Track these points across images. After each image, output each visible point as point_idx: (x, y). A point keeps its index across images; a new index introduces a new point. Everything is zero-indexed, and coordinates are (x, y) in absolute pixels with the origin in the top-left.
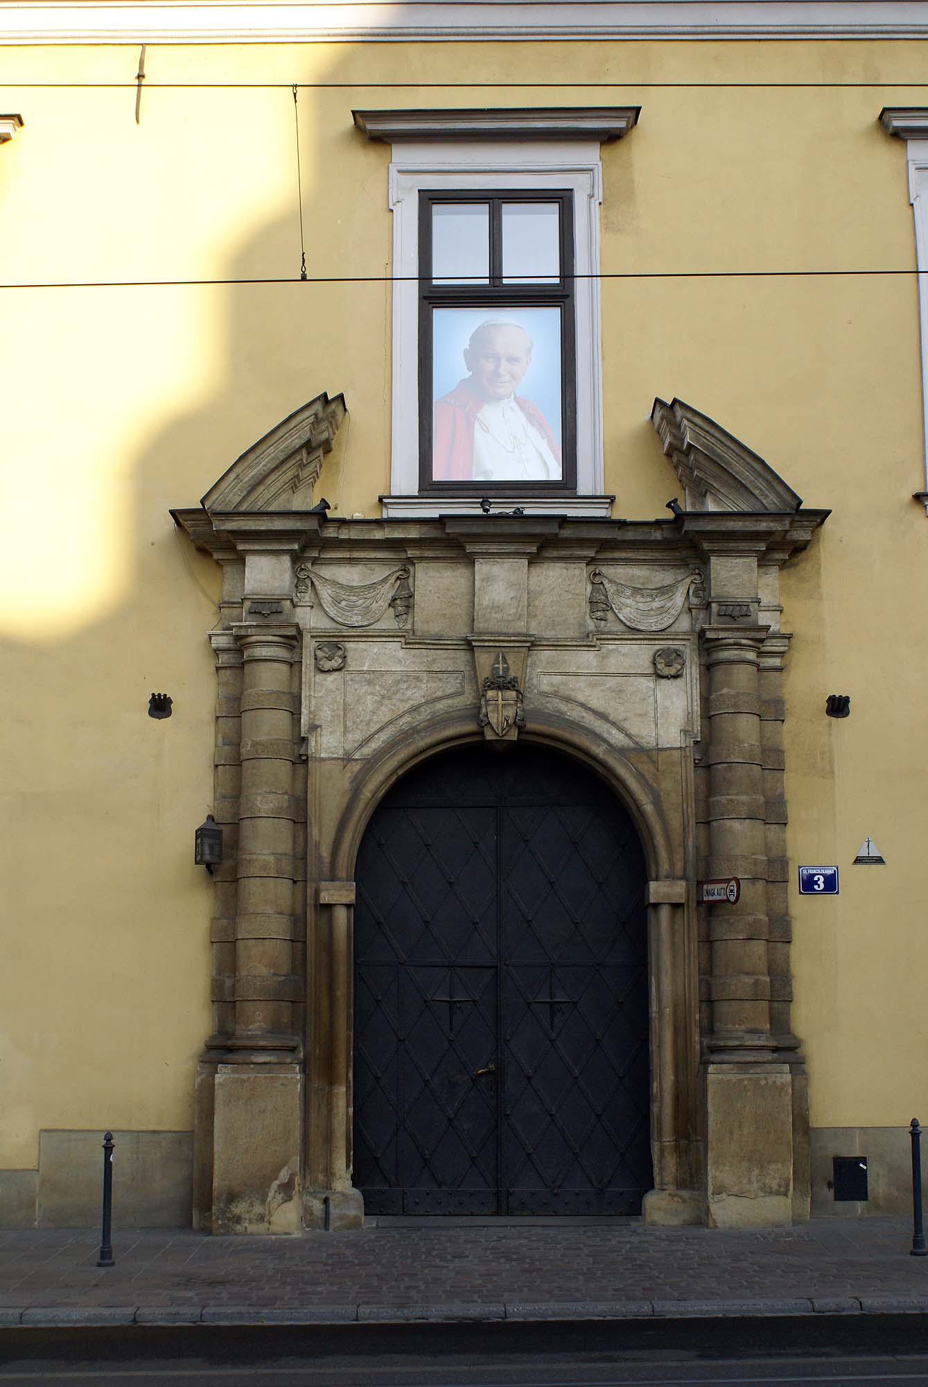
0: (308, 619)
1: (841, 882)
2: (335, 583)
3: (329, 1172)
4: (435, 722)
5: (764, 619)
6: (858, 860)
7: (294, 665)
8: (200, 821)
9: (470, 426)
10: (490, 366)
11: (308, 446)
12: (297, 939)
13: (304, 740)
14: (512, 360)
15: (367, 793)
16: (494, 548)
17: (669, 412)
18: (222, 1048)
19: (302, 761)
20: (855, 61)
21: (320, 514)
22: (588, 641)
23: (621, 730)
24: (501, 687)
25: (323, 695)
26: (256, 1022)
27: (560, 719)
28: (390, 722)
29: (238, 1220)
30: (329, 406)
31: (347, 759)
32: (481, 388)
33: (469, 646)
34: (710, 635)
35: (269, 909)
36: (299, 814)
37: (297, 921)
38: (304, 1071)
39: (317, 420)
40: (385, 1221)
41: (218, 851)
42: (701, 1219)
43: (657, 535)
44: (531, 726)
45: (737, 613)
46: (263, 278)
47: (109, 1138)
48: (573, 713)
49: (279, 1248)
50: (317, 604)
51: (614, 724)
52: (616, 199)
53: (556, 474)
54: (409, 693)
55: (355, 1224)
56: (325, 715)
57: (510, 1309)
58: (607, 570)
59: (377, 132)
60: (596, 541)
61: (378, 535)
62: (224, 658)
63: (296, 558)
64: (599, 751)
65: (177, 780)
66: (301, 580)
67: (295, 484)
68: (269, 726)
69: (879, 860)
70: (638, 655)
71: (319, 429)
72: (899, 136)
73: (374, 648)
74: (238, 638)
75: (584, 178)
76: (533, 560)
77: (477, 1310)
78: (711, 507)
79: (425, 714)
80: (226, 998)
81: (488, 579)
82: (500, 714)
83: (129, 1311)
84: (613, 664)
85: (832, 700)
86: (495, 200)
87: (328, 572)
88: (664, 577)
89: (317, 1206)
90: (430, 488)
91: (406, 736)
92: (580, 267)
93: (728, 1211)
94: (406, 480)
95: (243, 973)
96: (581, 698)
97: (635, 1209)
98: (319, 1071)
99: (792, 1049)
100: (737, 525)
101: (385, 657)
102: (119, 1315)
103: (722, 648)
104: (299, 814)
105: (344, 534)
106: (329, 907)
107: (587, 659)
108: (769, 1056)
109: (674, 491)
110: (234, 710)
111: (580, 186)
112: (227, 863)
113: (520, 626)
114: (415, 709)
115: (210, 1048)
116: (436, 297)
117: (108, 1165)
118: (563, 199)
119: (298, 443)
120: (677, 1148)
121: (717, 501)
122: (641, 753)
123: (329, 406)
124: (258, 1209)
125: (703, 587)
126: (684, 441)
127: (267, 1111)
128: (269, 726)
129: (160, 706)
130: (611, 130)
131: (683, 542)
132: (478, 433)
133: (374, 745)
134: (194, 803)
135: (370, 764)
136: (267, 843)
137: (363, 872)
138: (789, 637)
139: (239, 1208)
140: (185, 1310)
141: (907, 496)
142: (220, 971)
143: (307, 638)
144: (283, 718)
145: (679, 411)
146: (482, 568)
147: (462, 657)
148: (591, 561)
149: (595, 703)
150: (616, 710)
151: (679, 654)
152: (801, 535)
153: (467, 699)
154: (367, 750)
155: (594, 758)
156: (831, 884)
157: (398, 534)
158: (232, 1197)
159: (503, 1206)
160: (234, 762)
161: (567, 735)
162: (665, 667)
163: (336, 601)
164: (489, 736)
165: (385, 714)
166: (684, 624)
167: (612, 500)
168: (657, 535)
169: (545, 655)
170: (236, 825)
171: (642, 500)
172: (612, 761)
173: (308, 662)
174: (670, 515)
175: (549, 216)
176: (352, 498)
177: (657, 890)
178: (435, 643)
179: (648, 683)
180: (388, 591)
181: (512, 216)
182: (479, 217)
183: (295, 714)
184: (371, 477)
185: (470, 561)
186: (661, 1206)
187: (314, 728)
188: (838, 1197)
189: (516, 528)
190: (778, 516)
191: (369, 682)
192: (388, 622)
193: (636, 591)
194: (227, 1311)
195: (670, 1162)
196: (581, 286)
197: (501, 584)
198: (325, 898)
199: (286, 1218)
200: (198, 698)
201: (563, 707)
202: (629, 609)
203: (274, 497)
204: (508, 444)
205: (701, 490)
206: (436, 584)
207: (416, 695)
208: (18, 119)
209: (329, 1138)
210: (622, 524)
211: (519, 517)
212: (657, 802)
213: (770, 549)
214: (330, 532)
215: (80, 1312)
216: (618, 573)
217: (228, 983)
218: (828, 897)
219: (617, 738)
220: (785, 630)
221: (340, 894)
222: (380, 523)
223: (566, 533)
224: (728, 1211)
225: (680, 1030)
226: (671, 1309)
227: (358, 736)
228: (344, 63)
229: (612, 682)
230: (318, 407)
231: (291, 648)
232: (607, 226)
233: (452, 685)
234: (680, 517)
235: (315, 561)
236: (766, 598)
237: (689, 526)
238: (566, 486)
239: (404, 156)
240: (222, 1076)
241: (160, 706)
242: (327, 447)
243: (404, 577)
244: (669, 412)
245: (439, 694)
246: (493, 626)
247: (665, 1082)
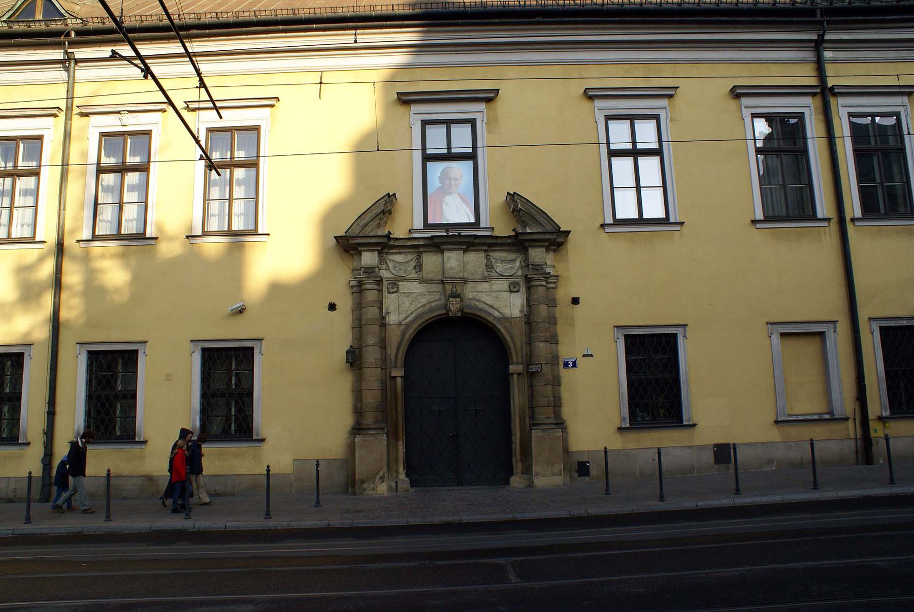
0: (385, 274)
2: (393, 261)
3: (397, 472)
4: (431, 310)
5: (548, 270)
6: (584, 356)
7: (380, 291)
8: (347, 348)
9: (441, 204)
10: (447, 182)
11: (383, 212)
12: (384, 389)
13: (384, 318)
14: (456, 179)
15: (407, 336)
16: (450, 247)
17: (513, 197)
18: (358, 429)
19: (383, 325)
20: (575, 71)
21: (388, 237)
22: (485, 279)
23: (498, 311)
24: (454, 297)
25: (390, 301)
26: (369, 419)
27: (476, 308)
29: (365, 490)
30: (390, 198)
31: (400, 324)
32: (445, 190)
33: (443, 282)
35: (373, 379)
36: (383, 344)
37: (384, 382)
38: (387, 436)
39: (386, 203)
40: (417, 489)
41: (354, 358)
42: (531, 485)
43: (509, 241)
44: (465, 311)
45: (539, 268)
46: (367, 151)
47: (318, 461)
48: (481, 306)
49: (381, 499)
50: (388, 269)
51: (496, 309)
52: (492, 122)
53: (473, 220)
55: (407, 490)
56: (391, 308)
57: (463, 518)
58: (492, 254)
59: (405, 100)
60: (486, 243)
61: (409, 243)
62: (355, 289)
63: (380, 253)
64: (490, 319)
65: (338, 333)
66: (382, 260)
67: (379, 226)
68: (372, 313)
69: (591, 356)
70: (504, 284)
71: (386, 206)
72: (591, 98)
73: (409, 284)
74: (360, 281)
75: (480, 114)
76: (465, 251)
77: (450, 519)
78: (529, 231)
79: (427, 307)
80: (358, 411)
81: (449, 258)
82: (454, 306)
83: (327, 522)
84: (495, 288)
85: (573, 298)
86: (448, 123)
87: (391, 257)
88: (512, 256)
89: (393, 484)
90: (427, 226)
92: (479, 144)
93: (541, 482)
94: (418, 224)
95: (364, 402)
97: (507, 482)
98: (393, 436)
99: (562, 424)
100: (538, 237)
101: (414, 287)
102: (323, 523)
103: (534, 281)
104: (383, 344)
105: (397, 244)
106: (395, 378)
107: (485, 286)
108: (554, 426)
109: (515, 225)
110: (358, 308)
111: (478, 116)
112: (358, 363)
113: (461, 275)
114: (424, 306)
115: (353, 429)
116: (427, 158)
117: (318, 471)
118: (473, 122)
119: (379, 211)
120: (522, 460)
121: (530, 228)
122: (505, 319)
123: (390, 198)
124: (372, 486)
125: (526, 259)
126: (518, 207)
127: (375, 451)
128: (372, 313)
129: (332, 307)
130: (489, 97)
131: (518, 244)
132: (444, 205)
133: (409, 319)
134: (344, 341)
135: (408, 326)
136: (371, 355)
137: (407, 364)
138: (557, 276)
139: (365, 486)
140: (347, 521)
141: (598, 225)
142: (356, 402)
143: (384, 281)
144: (376, 310)
145: (516, 197)
146: (447, 254)
147: (440, 287)
148: (486, 251)
149: (488, 302)
150: (497, 305)
151: (518, 284)
152: (561, 240)
153: (443, 302)
154: (407, 321)
155: (489, 322)
157: (416, 243)
158: (363, 482)
159: (460, 483)
160: (359, 326)
161: (479, 314)
162: (513, 288)
163: (394, 267)
164: (451, 315)
165: (413, 308)
166: (520, 273)
167: (493, 228)
168: (509, 241)
169: (470, 285)
170: (360, 349)
171: (503, 229)
172: (495, 323)
173: (385, 290)
174: (513, 234)
175: (468, 129)
176: (399, 230)
177: (512, 368)
178: (430, 281)
179: (508, 294)
180: (413, 264)
181: (455, 129)
182: (443, 129)
183: (381, 309)
184: (406, 222)
185: (442, 252)
186: (516, 481)
187: (388, 313)
188: (579, 476)
189: (458, 240)
190: (552, 233)
192: (413, 275)
193: (502, 261)
194: (362, 521)
195: (519, 465)
196: (480, 151)
197: (454, 260)
198: (393, 374)
199: (382, 489)
200: (345, 303)
201: (477, 303)
202: (500, 268)
203: (371, 230)
204: (455, 210)
205: (524, 224)
206: (430, 261)
207: (424, 301)
208: (277, 99)
209: (397, 460)
210: (497, 237)
211: (459, 235)
212: (512, 337)
213: (550, 245)
214: (392, 243)
215: (309, 522)
216: (495, 255)
217: (359, 406)
219: (496, 314)
220: (556, 274)
221: (398, 373)
222: (410, 239)
223: (477, 241)
224: (541, 482)
225: (522, 418)
226: (520, 516)
227: (404, 316)
228: (394, 75)
229: (494, 294)
230: (386, 198)
231: (379, 285)
232: (489, 132)
233: (437, 296)
234: (517, 234)
235: (386, 253)
236: (549, 263)
237: (520, 237)
238: (476, 225)
239: (415, 108)
240: (358, 439)
241: (332, 307)
242: (390, 212)
243: (419, 258)
244: (513, 197)
246: (451, 275)
247: (517, 436)
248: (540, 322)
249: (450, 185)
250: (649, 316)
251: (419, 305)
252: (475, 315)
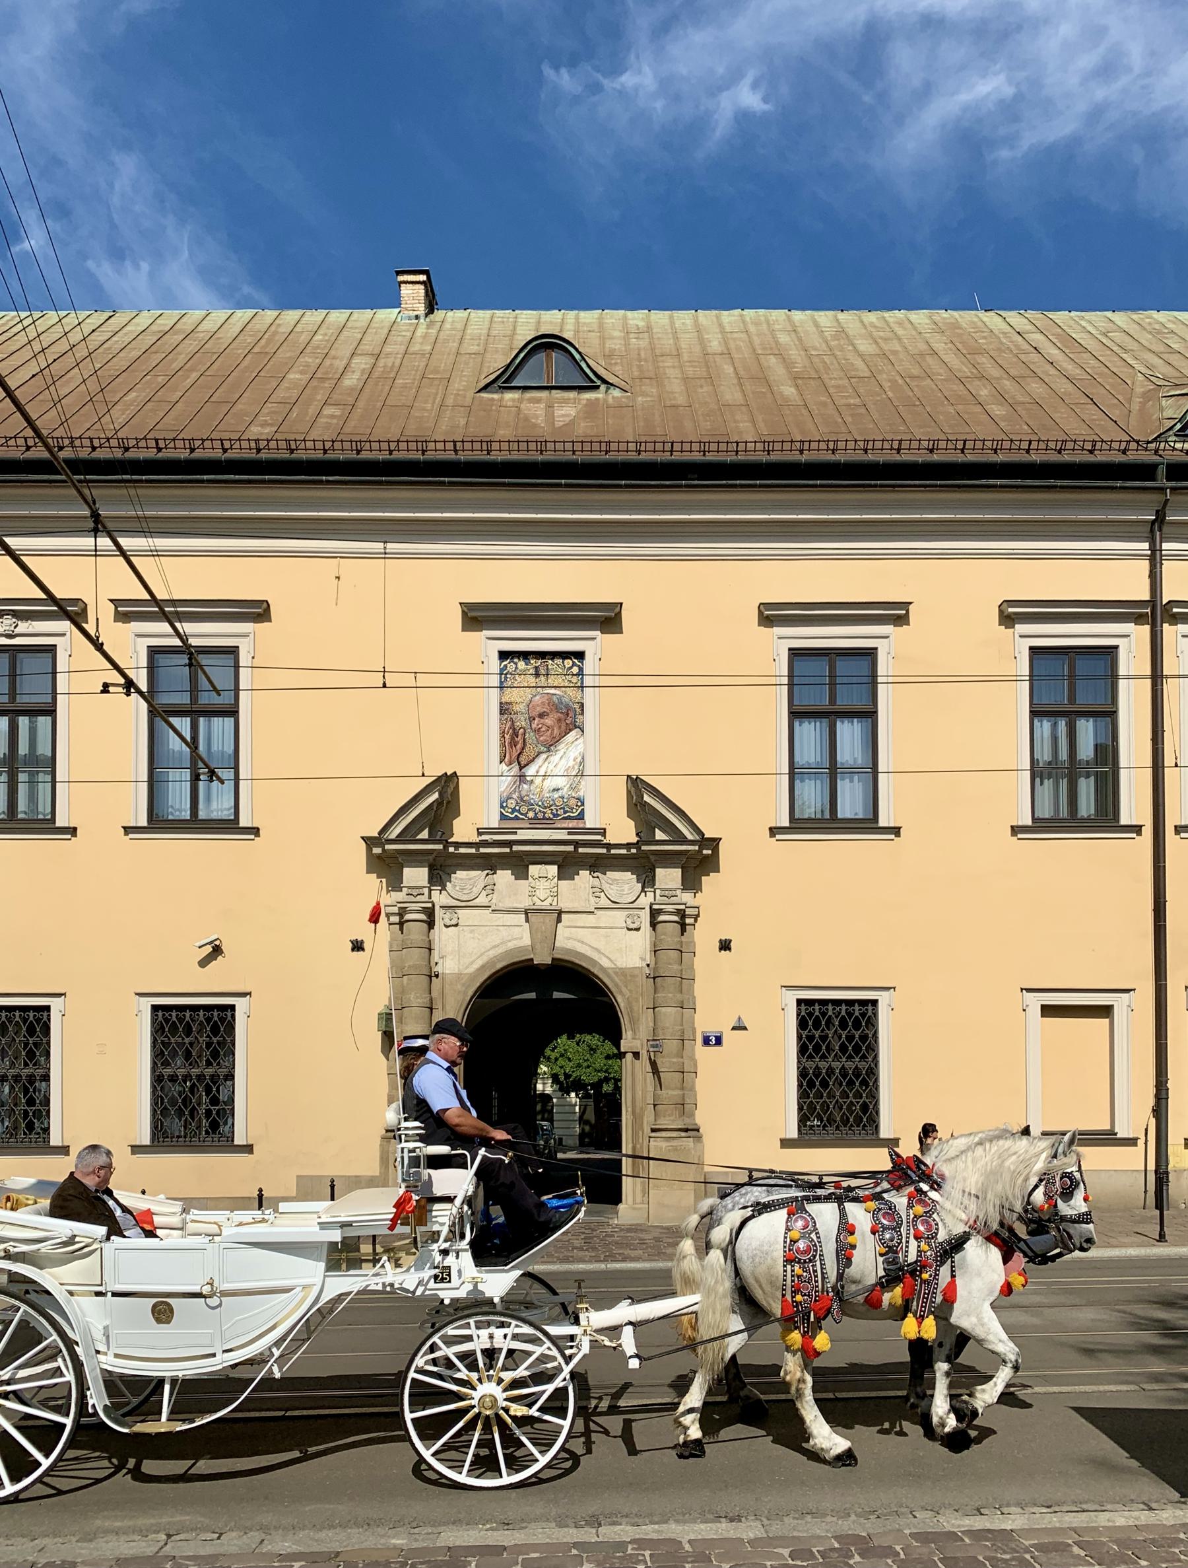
6: (734, 1028)
34: (655, 907)
69: (745, 1028)
91: (491, 962)
99: (698, 1130)
134: (380, 995)
135: (473, 976)
156: (719, 1041)
160: (399, 974)
191: (472, 932)
210: (609, 846)
220: (696, 904)
248: (669, 975)
250: (837, 976)
252: (572, 963)
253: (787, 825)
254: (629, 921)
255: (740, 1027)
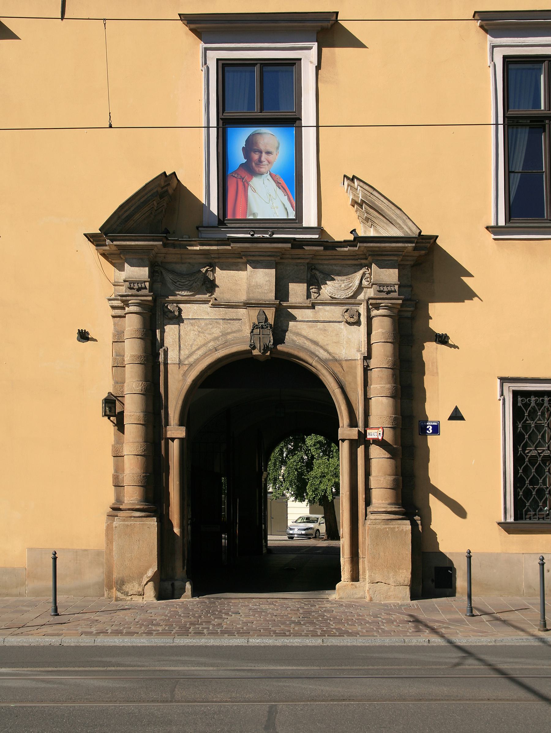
1: (442, 429)
6: (451, 418)
10: (256, 156)
14: (268, 153)
23: (326, 350)
28: (204, 345)
32: (251, 169)
51: (321, 347)
54: (214, 330)
96: (304, 333)
114: (216, 339)
149: (311, 336)
154: (191, 360)
165: (200, 341)
174: (351, 237)
191: (192, 325)
218: (435, 437)
219: (323, 354)
227: (187, 352)
245: (229, 330)
249: (260, 161)
251: (210, 337)
253: (504, 225)
254: (347, 315)
255: (456, 416)
